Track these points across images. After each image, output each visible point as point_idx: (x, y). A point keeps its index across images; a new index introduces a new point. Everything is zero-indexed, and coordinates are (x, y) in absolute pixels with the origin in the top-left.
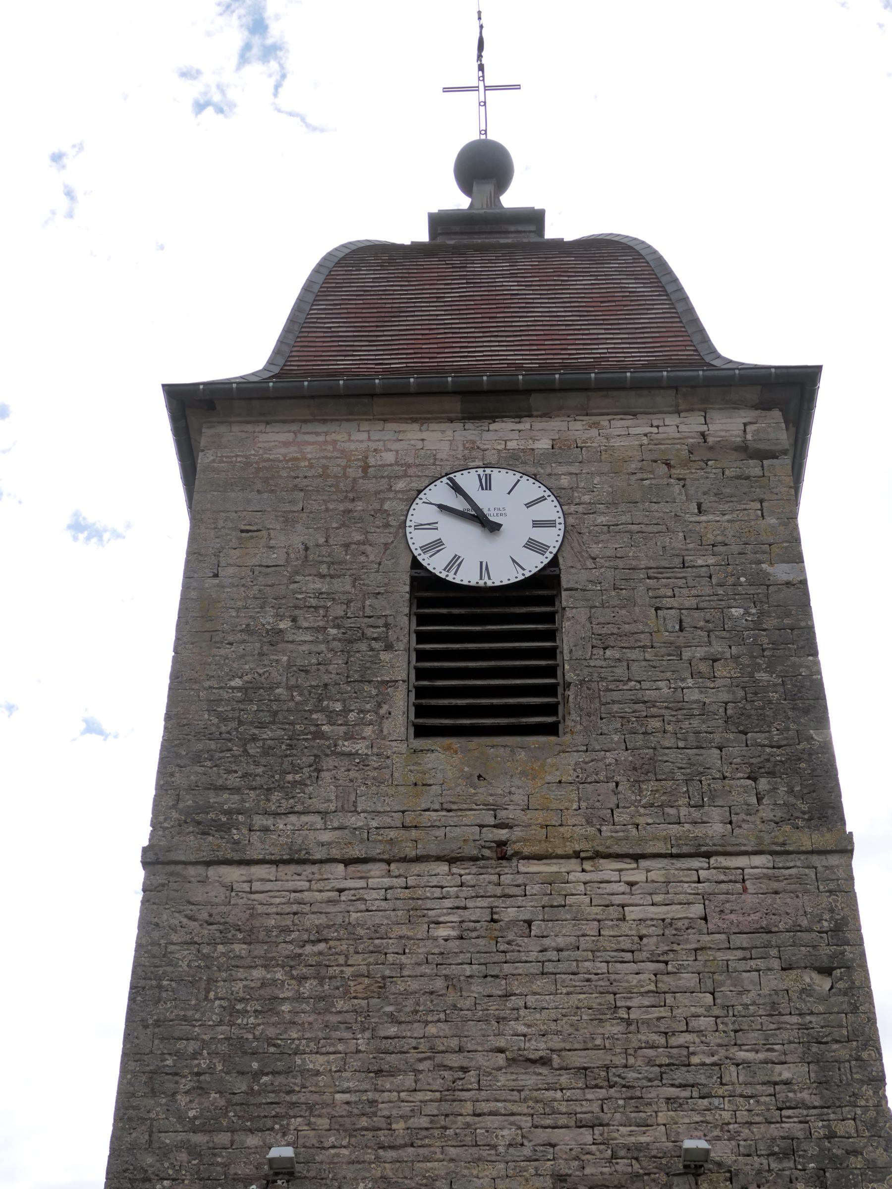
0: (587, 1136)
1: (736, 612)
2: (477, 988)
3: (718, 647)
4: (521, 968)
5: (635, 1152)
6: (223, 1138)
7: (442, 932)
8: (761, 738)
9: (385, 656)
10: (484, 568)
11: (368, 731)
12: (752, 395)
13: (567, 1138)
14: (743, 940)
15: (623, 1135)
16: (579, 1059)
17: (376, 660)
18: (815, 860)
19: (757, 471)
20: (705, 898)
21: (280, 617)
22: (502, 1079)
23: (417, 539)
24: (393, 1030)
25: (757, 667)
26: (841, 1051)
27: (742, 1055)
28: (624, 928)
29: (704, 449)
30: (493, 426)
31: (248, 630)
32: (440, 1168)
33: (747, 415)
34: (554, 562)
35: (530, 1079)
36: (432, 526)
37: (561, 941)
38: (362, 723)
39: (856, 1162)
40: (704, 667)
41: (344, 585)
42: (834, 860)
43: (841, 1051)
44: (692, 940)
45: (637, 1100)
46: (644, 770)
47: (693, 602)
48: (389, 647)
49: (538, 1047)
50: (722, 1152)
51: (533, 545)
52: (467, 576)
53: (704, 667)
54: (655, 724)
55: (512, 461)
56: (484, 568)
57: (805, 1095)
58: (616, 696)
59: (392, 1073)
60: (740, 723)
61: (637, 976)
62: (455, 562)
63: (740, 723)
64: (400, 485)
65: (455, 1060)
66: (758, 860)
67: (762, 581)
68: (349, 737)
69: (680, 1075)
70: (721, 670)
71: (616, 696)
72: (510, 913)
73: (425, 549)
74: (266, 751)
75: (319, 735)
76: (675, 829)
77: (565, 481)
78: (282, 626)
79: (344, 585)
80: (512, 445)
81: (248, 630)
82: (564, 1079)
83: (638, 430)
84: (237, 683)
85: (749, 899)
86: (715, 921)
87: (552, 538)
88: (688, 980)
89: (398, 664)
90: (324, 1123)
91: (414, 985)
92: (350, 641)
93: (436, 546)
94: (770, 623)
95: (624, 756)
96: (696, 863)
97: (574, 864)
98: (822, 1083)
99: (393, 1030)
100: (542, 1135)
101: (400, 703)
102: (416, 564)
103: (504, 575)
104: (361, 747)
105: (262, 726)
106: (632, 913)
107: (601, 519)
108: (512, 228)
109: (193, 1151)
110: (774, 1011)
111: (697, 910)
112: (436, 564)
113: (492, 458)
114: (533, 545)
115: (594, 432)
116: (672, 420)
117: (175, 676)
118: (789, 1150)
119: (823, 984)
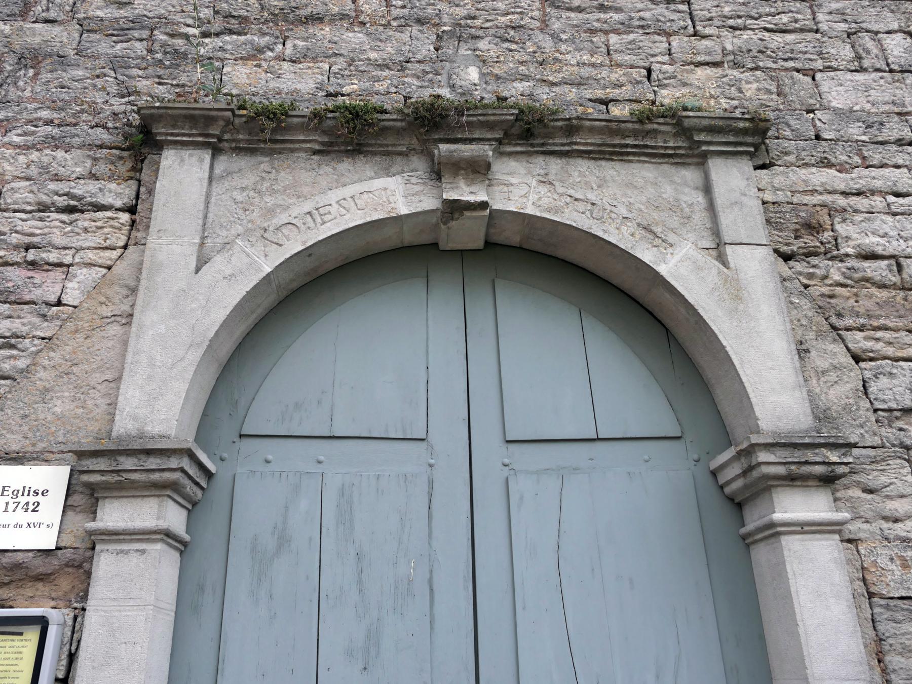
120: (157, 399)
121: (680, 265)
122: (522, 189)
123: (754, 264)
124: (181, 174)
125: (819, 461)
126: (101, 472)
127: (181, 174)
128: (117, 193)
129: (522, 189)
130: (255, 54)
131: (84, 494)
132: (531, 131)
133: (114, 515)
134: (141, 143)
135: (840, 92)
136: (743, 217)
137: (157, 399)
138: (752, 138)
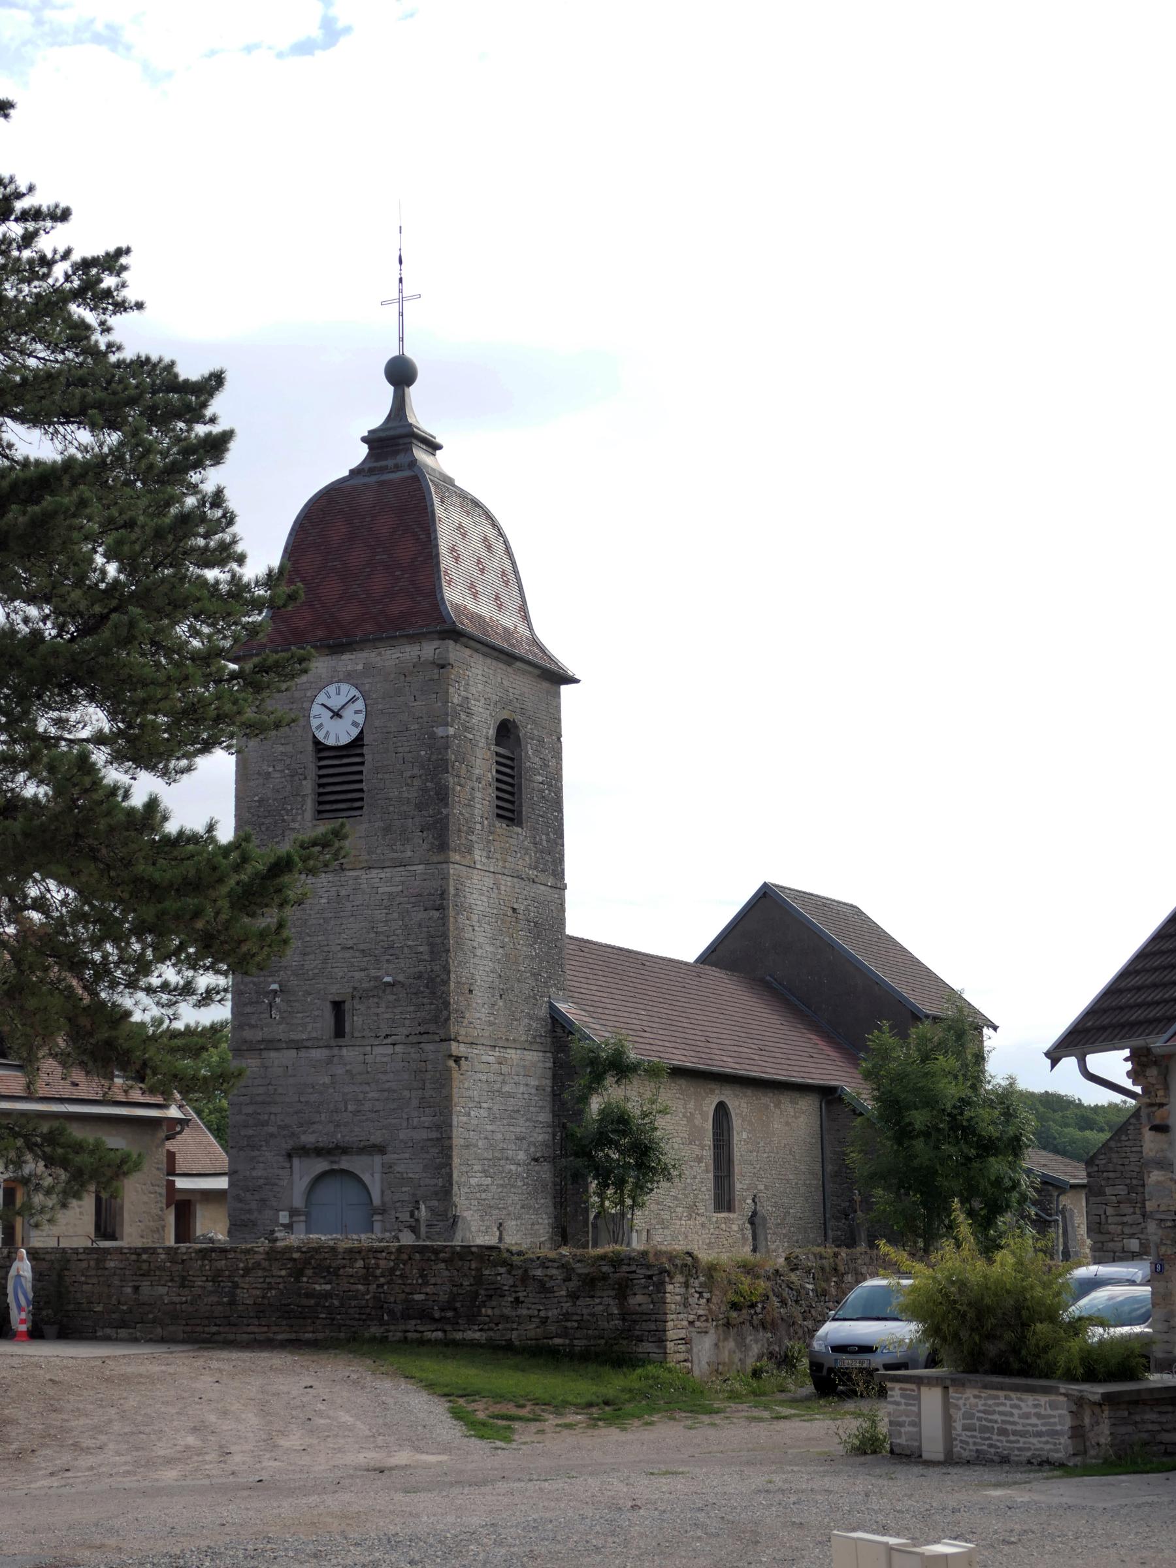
0: (363, 974)
1: (423, 753)
2: (332, 923)
3: (416, 771)
4: (345, 914)
5: (377, 978)
6: (262, 979)
7: (323, 901)
8: (425, 813)
9: (304, 782)
10: (337, 737)
11: (299, 818)
12: (436, 636)
13: (358, 975)
14: (413, 900)
15: (373, 973)
16: (362, 947)
17: (301, 785)
18: (439, 866)
19: (436, 677)
20: (403, 883)
21: (269, 766)
22: (340, 955)
23: (314, 723)
24: (308, 939)
25: (427, 780)
26: (438, 940)
27: (410, 943)
28: (378, 897)
29: (419, 664)
30: (343, 657)
31: (259, 773)
32: (322, 986)
33: (436, 644)
34: (362, 732)
35: (348, 954)
36: (318, 716)
37: (358, 903)
38: (297, 814)
39: (438, 980)
40: (409, 781)
41: (289, 748)
42: (444, 866)
43: (438, 940)
44: (399, 900)
45: (377, 961)
46: (387, 830)
47: (407, 749)
48: (305, 778)
49: (350, 943)
50: (401, 978)
51: (355, 724)
52: (331, 742)
53: (409, 781)
54: (391, 809)
55: (349, 678)
56: (337, 737)
57: (426, 957)
58: (379, 796)
59: (308, 954)
60: (419, 807)
61: (380, 915)
62: (327, 734)
63: (419, 807)
64: (309, 694)
65: (326, 949)
66: (421, 867)
67: (433, 736)
68: (293, 821)
69: (391, 951)
70: (417, 782)
71: (379, 796)
72: (343, 893)
73: (317, 728)
74: (267, 829)
75: (284, 821)
76: (395, 855)
77: (367, 687)
78: (271, 769)
79: (289, 748)
80: (349, 668)
81: (259, 773)
82: (357, 954)
83: (395, 656)
84: (256, 798)
85: (417, 883)
86: (405, 892)
87: (360, 719)
88: (395, 915)
89: (308, 787)
90: (289, 973)
91: (314, 922)
92: (292, 776)
93: (320, 726)
94: (434, 757)
95: (381, 824)
96: (402, 869)
97: (363, 872)
98: (432, 952)
99: (308, 939)
100: (350, 974)
101: (309, 805)
102: (314, 737)
103: (345, 740)
104: (296, 825)
105: (265, 817)
106: (380, 890)
107: (380, 706)
108: (401, 441)
109: (255, 984)
110: (420, 926)
111: (400, 888)
112: (320, 736)
113: (341, 677)
114: (355, 724)
115: (379, 658)
116: (408, 649)
117: (236, 797)
118: (419, 976)
119: (436, 914)
120: (298, 1202)
121: (366, 1178)
122: (345, 1163)
123: (377, 1176)
124: (296, 1161)
125: (383, 1211)
126: (293, 1212)
127: (296, 1161)
128: (288, 1165)
129: (345, 1163)
130: (304, 1133)
131: (291, 1217)
132: (344, 1150)
133: (295, 1219)
134: (289, 1156)
135: (402, 1136)
136: (378, 1167)
137: (298, 1202)
138: (380, 1149)
